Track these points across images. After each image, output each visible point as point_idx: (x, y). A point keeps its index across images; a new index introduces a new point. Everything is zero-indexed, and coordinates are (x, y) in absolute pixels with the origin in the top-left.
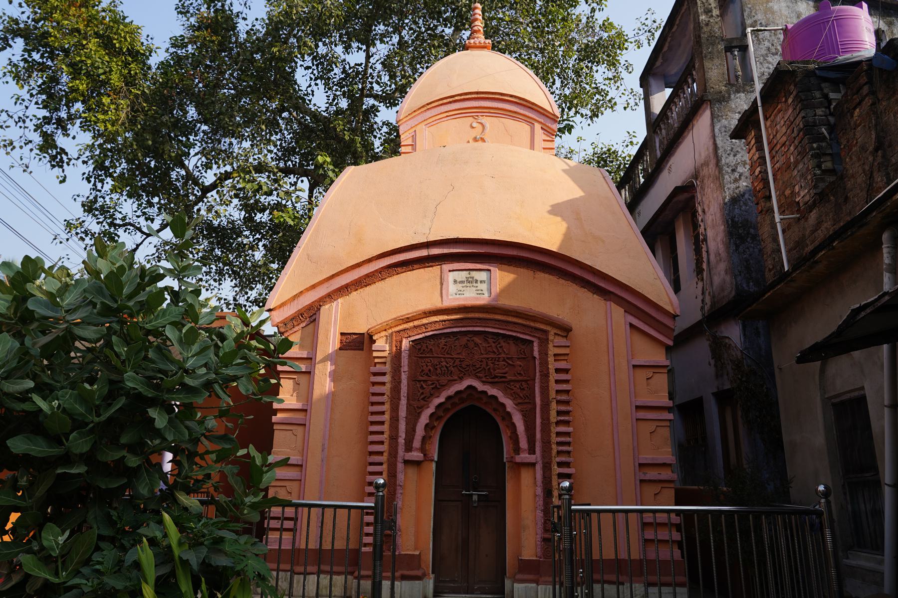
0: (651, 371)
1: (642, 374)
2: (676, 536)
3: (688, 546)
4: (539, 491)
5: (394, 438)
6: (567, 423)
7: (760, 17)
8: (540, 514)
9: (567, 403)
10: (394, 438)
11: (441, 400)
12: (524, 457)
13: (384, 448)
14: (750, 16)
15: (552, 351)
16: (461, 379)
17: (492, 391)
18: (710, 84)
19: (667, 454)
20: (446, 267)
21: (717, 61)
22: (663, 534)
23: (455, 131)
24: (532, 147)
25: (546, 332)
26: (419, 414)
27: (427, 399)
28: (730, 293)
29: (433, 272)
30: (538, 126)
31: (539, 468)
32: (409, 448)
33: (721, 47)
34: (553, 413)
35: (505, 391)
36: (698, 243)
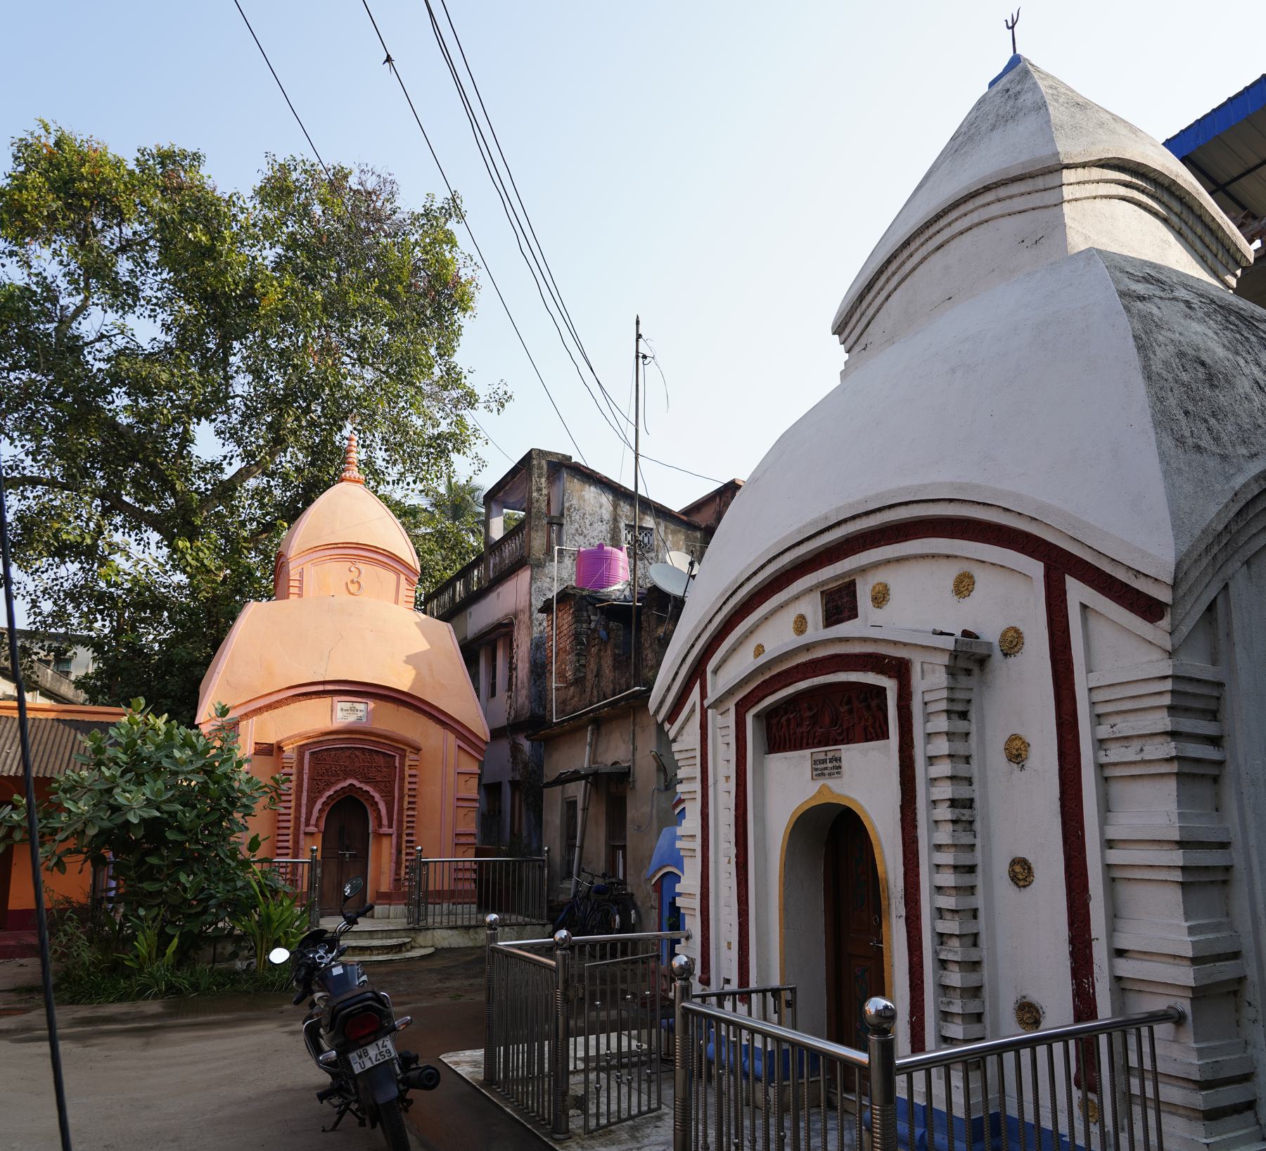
0: (467, 777)
1: (463, 778)
2: (474, 876)
3: (479, 882)
4: (394, 851)
5: (297, 818)
6: (413, 809)
7: (574, 502)
8: (393, 865)
9: (414, 796)
10: (297, 818)
11: (331, 792)
12: (385, 830)
13: (291, 824)
14: (569, 500)
15: (408, 763)
16: (345, 779)
17: (366, 788)
18: (533, 551)
19: (473, 828)
20: (336, 699)
21: (540, 534)
22: (467, 875)
23: (337, 572)
24: (396, 602)
25: (404, 750)
26: (315, 803)
27: (321, 792)
28: (526, 713)
29: (326, 701)
30: (403, 577)
31: (394, 837)
32: (307, 825)
33: (545, 522)
34: (406, 803)
35: (374, 788)
36: (512, 668)
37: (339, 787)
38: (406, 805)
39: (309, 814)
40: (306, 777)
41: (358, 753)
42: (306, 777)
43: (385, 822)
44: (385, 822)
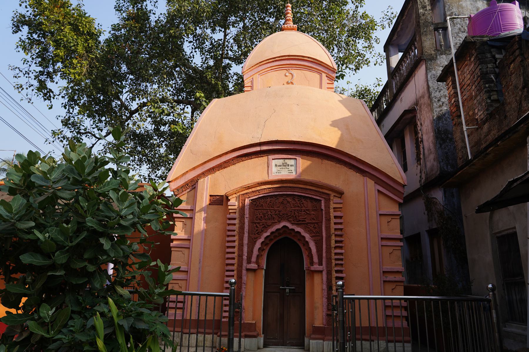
0: (389, 218)
1: (385, 219)
2: (405, 313)
3: (411, 319)
4: (325, 287)
5: (240, 256)
6: (341, 248)
7: (454, 10)
8: (325, 300)
9: (341, 236)
10: (240, 256)
11: (268, 234)
12: (316, 267)
13: (235, 261)
14: (449, 10)
15: (332, 206)
16: (279, 222)
17: (298, 229)
18: (425, 50)
19: (399, 266)
20: (271, 157)
21: (429, 37)
22: (397, 312)
23: (276, 78)
24: (321, 87)
25: (329, 195)
26: (255, 243)
27: (260, 234)
28: (436, 172)
29: (263, 160)
30: (324, 75)
31: (324, 274)
32: (249, 262)
33: (432, 28)
34: (333, 242)
35: (306, 229)
36: (418, 142)
37: (274, 229)
38: (333, 244)
39: (250, 253)
40: (246, 221)
41: (289, 199)
42: (246, 221)
43: (316, 259)
44: (316, 259)
